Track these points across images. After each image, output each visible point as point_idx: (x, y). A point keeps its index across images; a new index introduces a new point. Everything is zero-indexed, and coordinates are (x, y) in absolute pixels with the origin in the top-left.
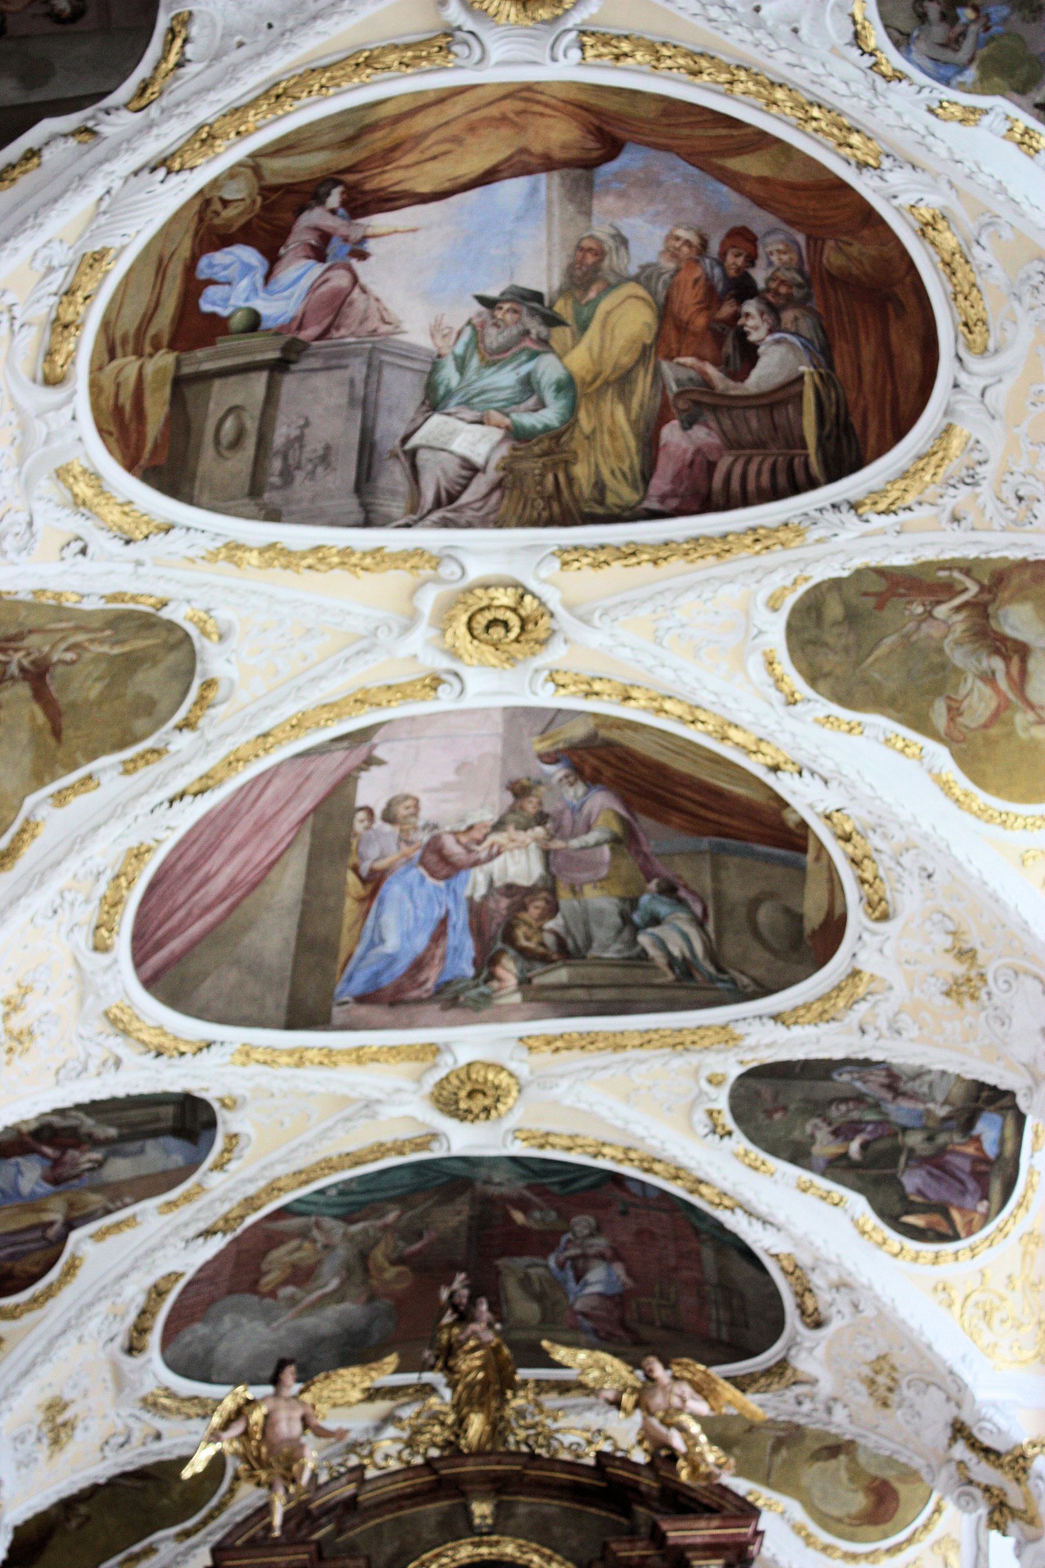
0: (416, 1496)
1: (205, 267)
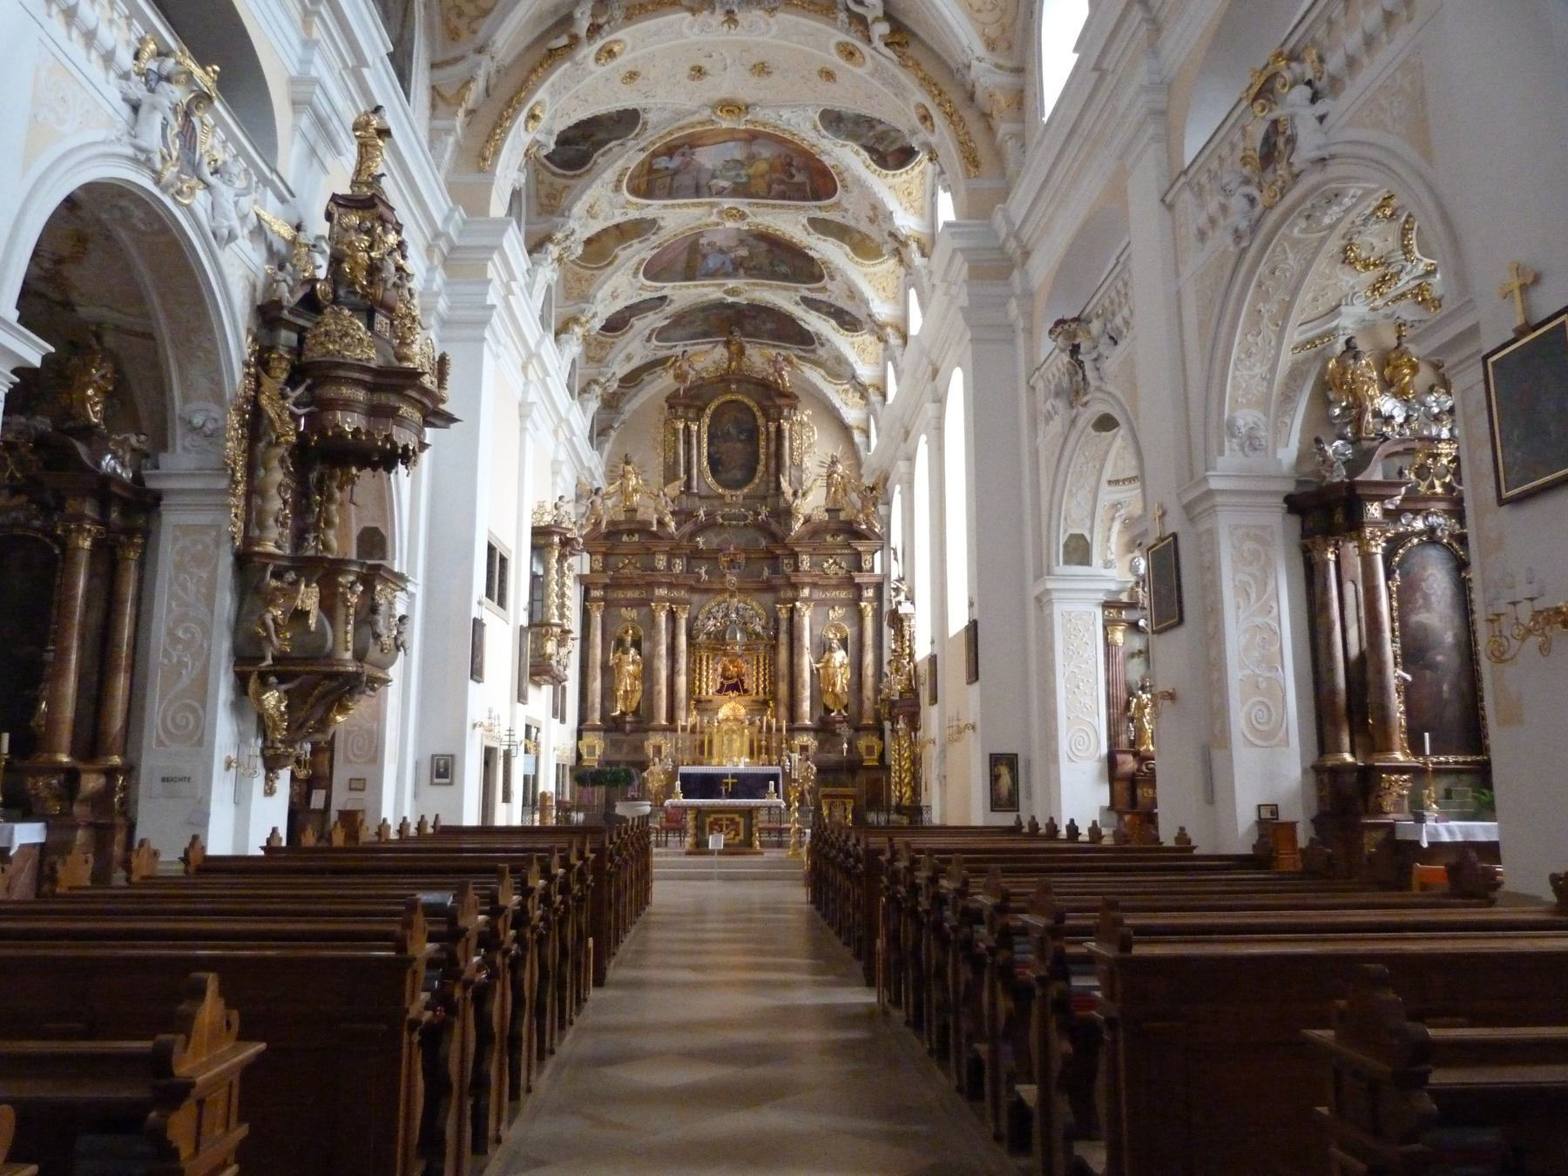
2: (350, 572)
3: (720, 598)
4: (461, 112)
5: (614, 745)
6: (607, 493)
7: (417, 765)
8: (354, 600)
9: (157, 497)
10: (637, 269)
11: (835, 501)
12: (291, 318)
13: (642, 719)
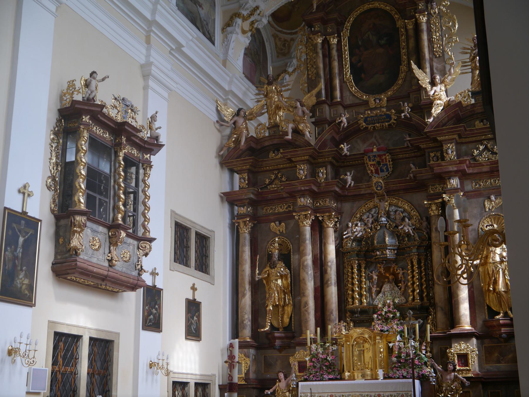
3: (371, 205)
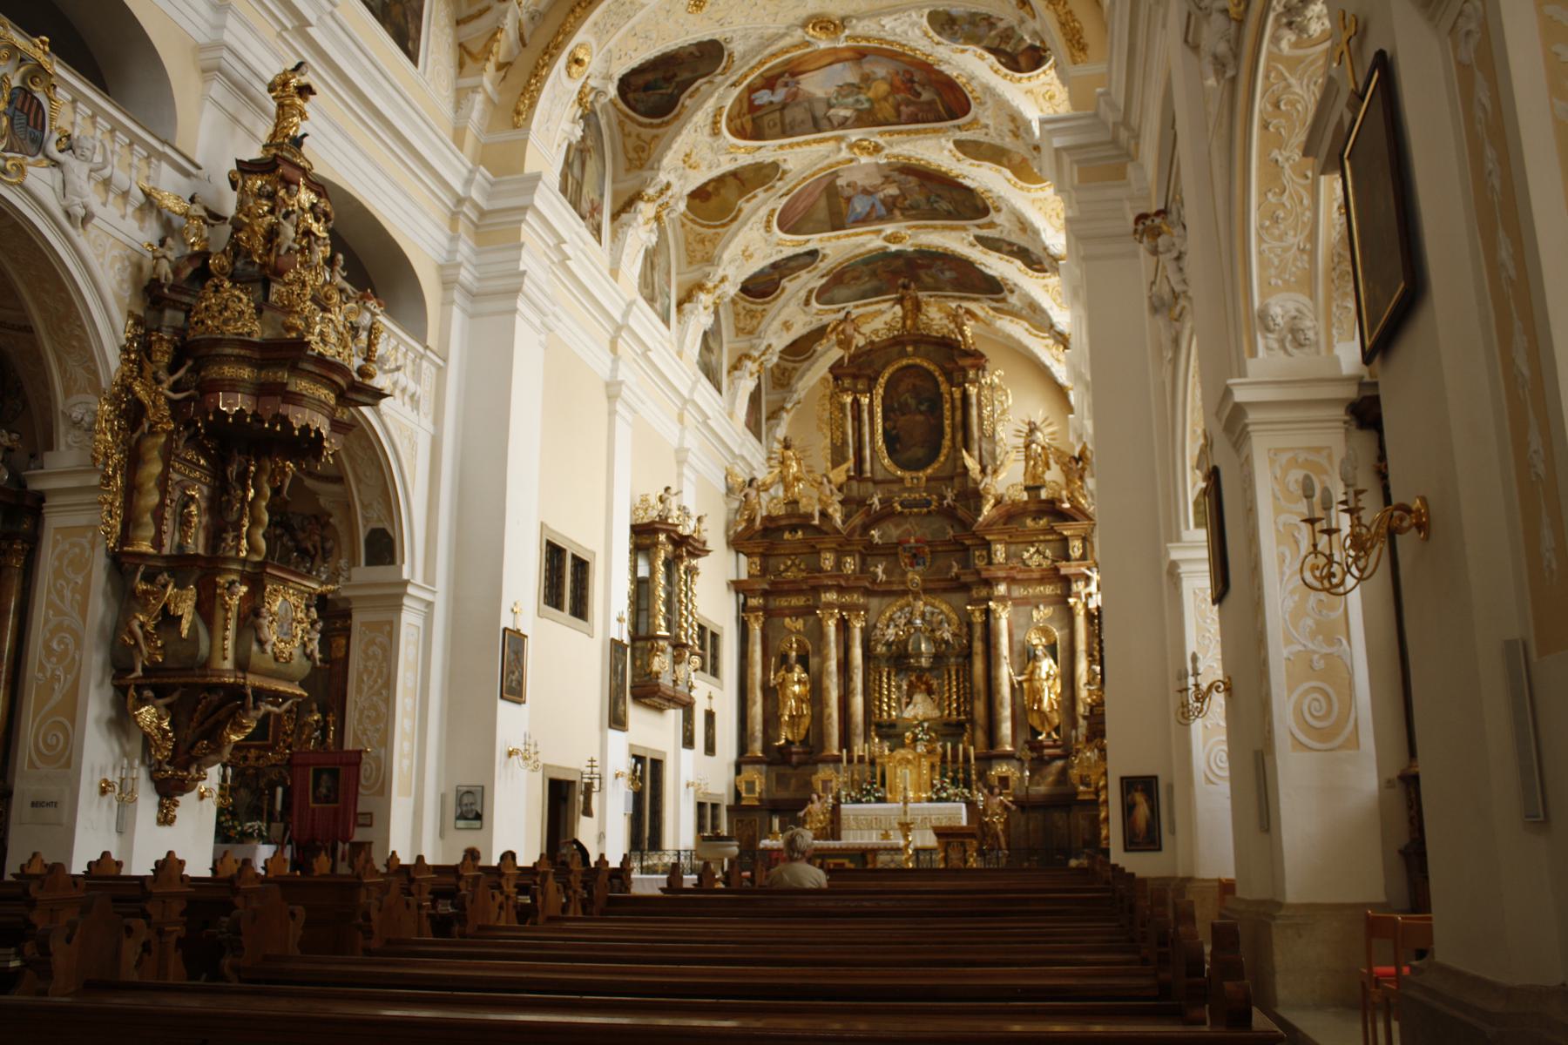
0: (891, 345)
1: (753, 97)
2: (230, 571)
3: (902, 602)
4: (490, 67)
5: (781, 780)
6: (764, 484)
7: (443, 798)
8: (235, 601)
9: (40, 497)
10: (768, 222)
11: (1034, 477)
12: (175, 296)
13: (812, 750)
